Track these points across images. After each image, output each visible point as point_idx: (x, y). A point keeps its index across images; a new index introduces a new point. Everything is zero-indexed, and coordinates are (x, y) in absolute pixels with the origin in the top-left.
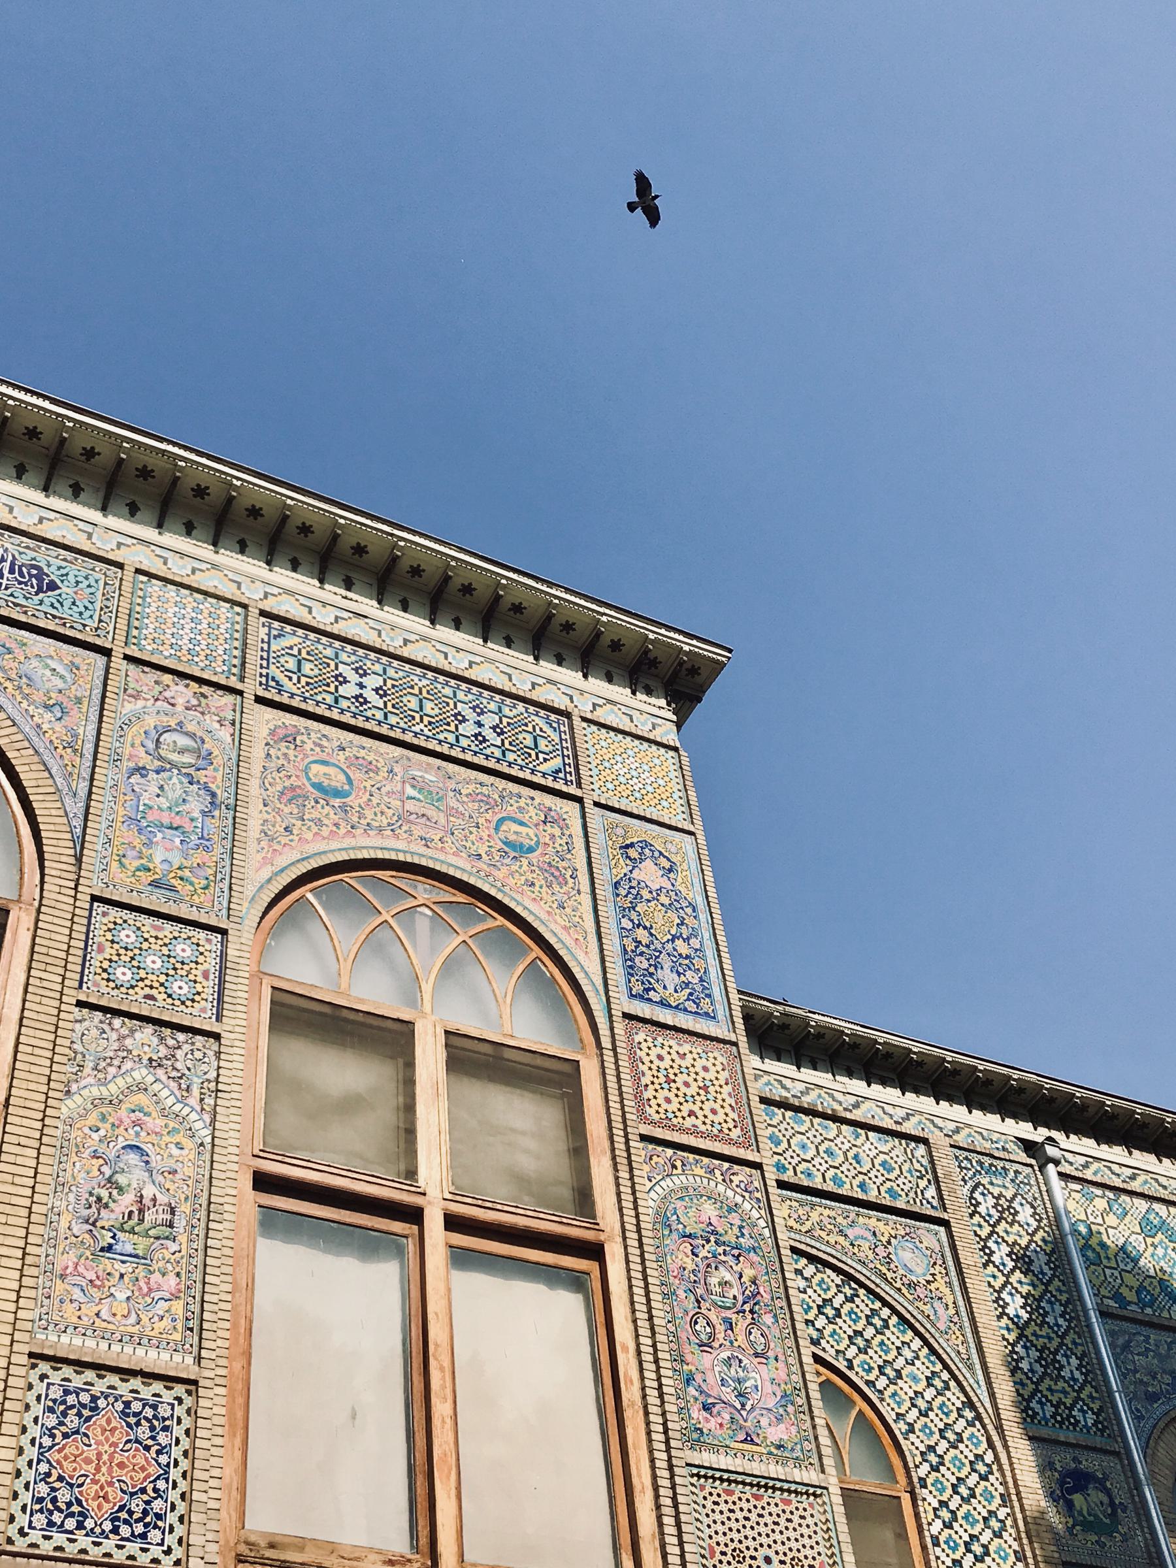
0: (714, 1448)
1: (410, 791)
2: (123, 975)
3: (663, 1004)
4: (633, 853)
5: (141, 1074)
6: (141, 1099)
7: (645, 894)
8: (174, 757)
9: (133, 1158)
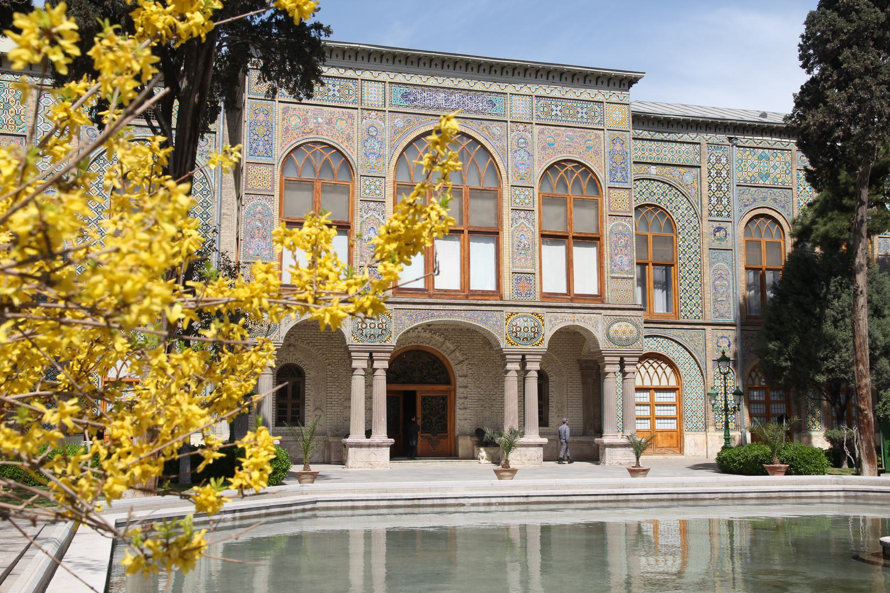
0: (615, 273)
2: (518, 201)
3: (617, 182)
4: (615, 142)
5: (522, 221)
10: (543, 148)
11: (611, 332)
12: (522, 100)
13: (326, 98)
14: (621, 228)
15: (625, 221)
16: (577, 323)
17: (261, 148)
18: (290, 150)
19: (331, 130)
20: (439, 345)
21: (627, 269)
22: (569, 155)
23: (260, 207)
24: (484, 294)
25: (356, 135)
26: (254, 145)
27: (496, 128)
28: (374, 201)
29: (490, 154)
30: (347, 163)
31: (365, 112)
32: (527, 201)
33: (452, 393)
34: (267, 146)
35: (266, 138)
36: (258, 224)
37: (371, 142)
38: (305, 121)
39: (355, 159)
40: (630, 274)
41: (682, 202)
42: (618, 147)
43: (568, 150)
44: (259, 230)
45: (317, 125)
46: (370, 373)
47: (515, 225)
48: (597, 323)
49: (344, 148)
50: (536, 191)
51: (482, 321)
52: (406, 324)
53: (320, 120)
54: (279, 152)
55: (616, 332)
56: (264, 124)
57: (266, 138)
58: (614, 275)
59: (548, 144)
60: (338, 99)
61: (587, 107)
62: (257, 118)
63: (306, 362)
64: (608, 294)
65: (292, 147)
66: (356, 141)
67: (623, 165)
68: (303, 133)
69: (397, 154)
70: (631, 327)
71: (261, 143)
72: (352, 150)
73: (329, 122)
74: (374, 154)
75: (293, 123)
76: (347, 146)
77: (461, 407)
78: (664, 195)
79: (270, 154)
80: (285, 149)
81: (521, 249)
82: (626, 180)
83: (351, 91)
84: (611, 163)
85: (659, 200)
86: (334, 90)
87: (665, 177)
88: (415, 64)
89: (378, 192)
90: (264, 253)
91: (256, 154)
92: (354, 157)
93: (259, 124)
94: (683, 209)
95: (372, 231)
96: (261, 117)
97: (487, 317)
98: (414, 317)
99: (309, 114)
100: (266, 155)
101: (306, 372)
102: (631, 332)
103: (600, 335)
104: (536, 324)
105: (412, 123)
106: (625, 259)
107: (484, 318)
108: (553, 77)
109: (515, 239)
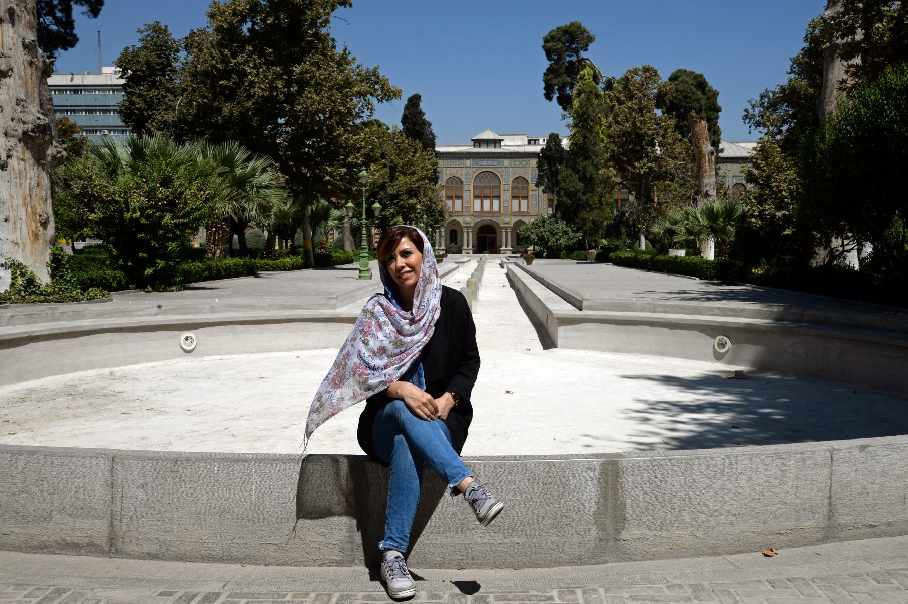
24: (496, 212)
27: (500, 169)
30: (462, 182)
46: (468, 232)
54: (445, 179)
64: (530, 211)
81: (506, 200)
92: (463, 180)
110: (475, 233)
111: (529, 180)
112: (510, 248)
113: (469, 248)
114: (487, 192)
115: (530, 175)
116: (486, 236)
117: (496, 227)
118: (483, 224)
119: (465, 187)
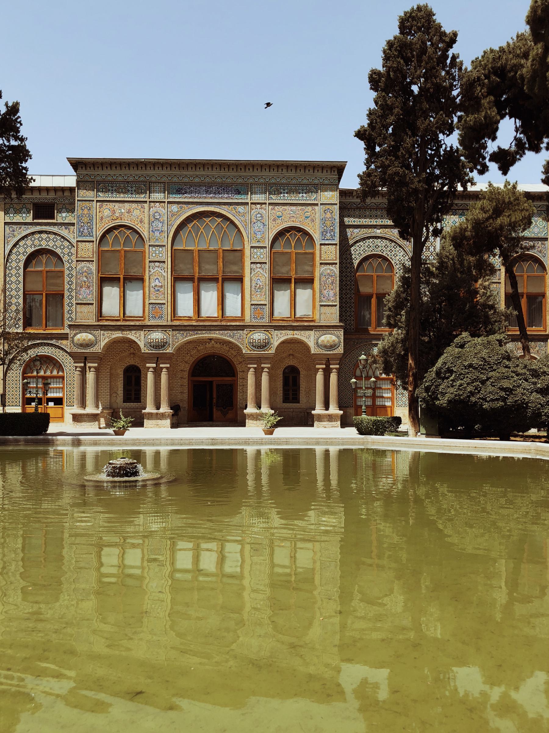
0: (324, 302)
1: (291, 212)
2: (255, 256)
4: (326, 212)
5: (259, 270)
6: (259, 273)
7: (327, 219)
8: (258, 219)
9: (258, 280)
10: (274, 220)
11: (320, 341)
12: (260, 188)
13: (298, 198)
14: (329, 271)
15: (332, 266)
16: (295, 336)
17: (86, 231)
18: (104, 231)
19: (130, 217)
20: (226, 352)
21: (333, 299)
22: (292, 223)
23: (85, 268)
25: (146, 219)
26: (81, 230)
27: (241, 209)
28: (158, 262)
29: (236, 226)
31: (152, 204)
32: (262, 256)
33: (236, 381)
34: (90, 230)
35: (89, 224)
36: (85, 279)
37: (156, 223)
38: (114, 212)
39: (146, 234)
40: (334, 302)
41: (400, 251)
42: (328, 215)
43: (292, 219)
44: (85, 283)
45: (121, 214)
47: (253, 273)
48: (309, 336)
49: (139, 228)
50: (268, 249)
51: (230, 336)
52: (180, 339)
53: (123, 211)
55: (323, 341)
56: (87, 216)
57: (89, 224)
58: (323, 304)
59: (278, 217)
60: (287, 198)
61: (306, 189)
62: (83, 212)
63: (142, 364)
65: (105, 229)
66: (146, 223)
67: (332, 228)
68: (112, 219)
69: (173, 230)
70: (334, 338)
71: (86, 228)
72: (144, 229)
73: (129, 212)
74: (158, 230)
75: (106, 214)
76: (140, 227)
77: (240, 391)
78: (386, 247)
79: (91, 234)
80: (101, 231)
82: (334, 238)
83: (143, 190)
84: (323, 226)
85: (382, 251)
86: (132, 191)
87: (387, 234)
88: (185, 168)
89: (161, 255)
90: (89, 297)
91: (83, 235)
92: (145, 234)
93: (84, 216)
94: (400, 256)
95: (157, 281)
96: (86, 211)
97: (234, 333)
98: (185, 334)
99: (116, 207)
100: (89, 235)
101: (142, 369)
102: (334, 341)
103: (311, 344)
104: (267, 337)
105: (183, 209)
106: (331, 293)
107: (232, 334)
108: (282, 170)
109: (253, 282)
110: (186, 375)
111: (317, 236)
112: (265, 409)
113: (162, 410)
114: (210, 270)
115: (318, 221)
116: (211, 382)
117: (235, 361)
118: (203, 351)
119: (152, 254)
